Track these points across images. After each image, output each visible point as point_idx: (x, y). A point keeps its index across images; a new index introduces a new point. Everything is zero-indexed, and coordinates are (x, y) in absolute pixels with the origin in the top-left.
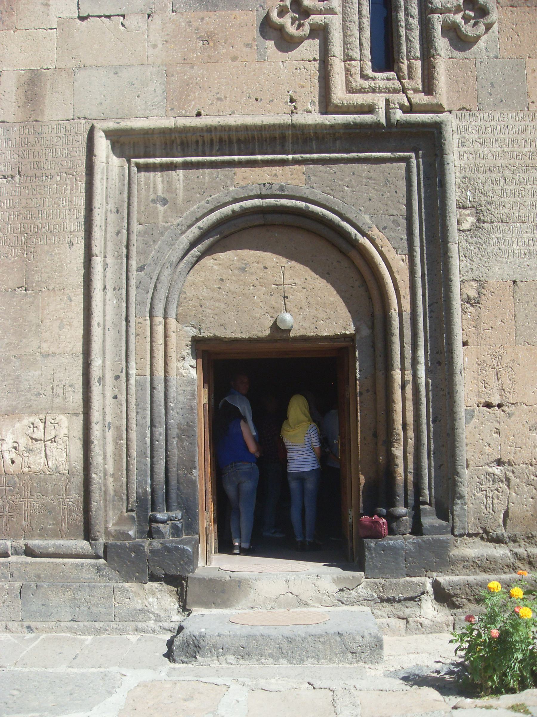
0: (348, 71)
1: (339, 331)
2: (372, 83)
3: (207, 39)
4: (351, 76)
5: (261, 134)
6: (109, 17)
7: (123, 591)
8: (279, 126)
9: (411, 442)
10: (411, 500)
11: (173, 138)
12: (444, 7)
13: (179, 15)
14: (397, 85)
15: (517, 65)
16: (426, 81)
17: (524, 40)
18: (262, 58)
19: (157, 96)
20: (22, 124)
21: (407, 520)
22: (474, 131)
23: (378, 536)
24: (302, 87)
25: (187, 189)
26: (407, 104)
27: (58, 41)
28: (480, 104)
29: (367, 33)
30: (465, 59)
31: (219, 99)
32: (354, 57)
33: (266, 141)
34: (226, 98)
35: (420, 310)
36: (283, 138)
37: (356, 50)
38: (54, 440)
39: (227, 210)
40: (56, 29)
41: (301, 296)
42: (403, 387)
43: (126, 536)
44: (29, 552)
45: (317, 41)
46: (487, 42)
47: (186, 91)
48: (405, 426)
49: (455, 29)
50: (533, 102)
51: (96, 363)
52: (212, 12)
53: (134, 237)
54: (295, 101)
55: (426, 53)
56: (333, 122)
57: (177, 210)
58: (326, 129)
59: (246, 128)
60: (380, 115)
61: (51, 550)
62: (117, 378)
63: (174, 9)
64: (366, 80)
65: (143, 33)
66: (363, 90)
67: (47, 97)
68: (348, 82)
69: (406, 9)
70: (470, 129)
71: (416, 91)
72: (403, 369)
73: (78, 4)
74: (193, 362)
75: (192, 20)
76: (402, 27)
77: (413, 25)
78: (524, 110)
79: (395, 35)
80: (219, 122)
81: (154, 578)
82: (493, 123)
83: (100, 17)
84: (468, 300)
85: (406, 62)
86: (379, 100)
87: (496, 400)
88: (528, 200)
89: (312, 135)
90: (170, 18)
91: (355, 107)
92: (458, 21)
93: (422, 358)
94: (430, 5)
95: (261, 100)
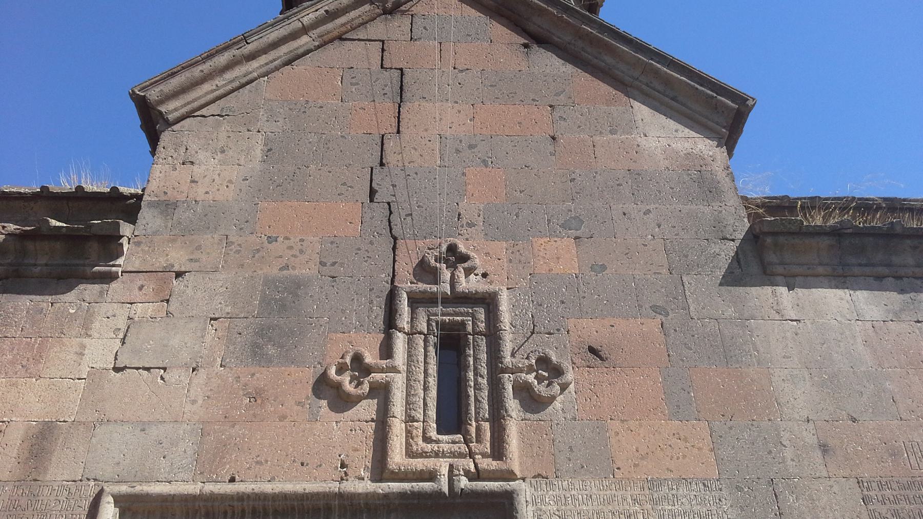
0: (409, 434)
3: (255, 396)
4: (413, 439)
5: (302, 504)
6: (148, 369)
8: (324, 495)
11: (197, 507)
12: (515, 367)
13: (228, 369)
14: (464, 448)
15: (598, 427)
16: (496, 444)
17: (604, 400)
18: (314, 418)
19: (187, 458)
20: (17, 484)
22: (551, 503)
24: (356, 450)
26: (472, 468)
27: (83, 392)
28: (558, 470)
29: (433, 393)
30: (540, 421)
31: (257, 463)
32: (416, 418)
33: (308, 511)
34: (267, 461)
37: (419, 410)
40: (85, 379)
45: (376, 401)
46: (563, 402)
47: (222, 452)
49: (528, 389)
50: (618, 468)
52: (265, 368)
54: (346, 466)
55: (496, 414)
56: (387, 490)
58: (379, 499)
59: (285, 496)
60: (443, 483)
63: (223, 363)
64: (428, 444)
65: (183, 388)
66: (424, 455)
67: (56, 453)
68: (408, 445)
69: (475, 369)
70: (547, 500)
71: (484, 455)
73: (116, 355)
75: (241, 376)
76: (471, 387)
77: (482, 385)
78: (610, 478)
79: (463, 395)
80: (253, 489)
82: (573, 492)
83: (137, 369)
85: (474, 424)
86: (441, 466)
89: (363, 506)
90: (218, 373)
91: (414, 473)
92: (530, 381)
94: (500, 365)
95: (307, 465)
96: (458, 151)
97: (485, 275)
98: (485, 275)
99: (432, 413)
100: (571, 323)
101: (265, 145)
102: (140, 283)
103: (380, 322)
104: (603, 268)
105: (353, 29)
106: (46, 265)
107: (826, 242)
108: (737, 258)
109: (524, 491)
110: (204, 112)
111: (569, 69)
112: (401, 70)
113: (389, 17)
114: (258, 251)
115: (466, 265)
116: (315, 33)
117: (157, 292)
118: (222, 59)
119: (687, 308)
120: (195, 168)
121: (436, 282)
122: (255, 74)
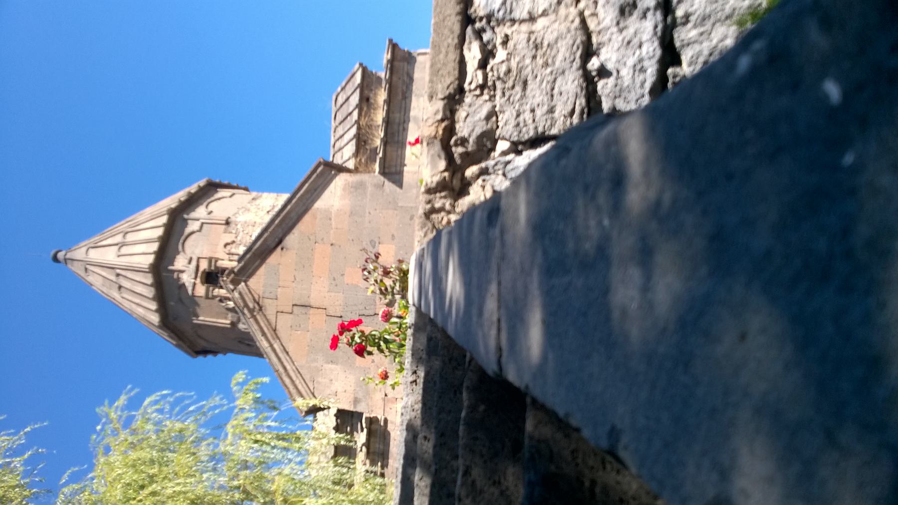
96: (336, 285)
101: (329, 363)
102: (389, 409)
104: (393, 236)
105: (270, 324)
106: (379, 444)
107: (389, 148)
108: (394, 182)
110: (312, 388)
112: (293, 305)
113: (263, 308)
114: (378, 366)
116: (272, 341)
117: (393, 402)
118: (287, 381)
119: (412, 207)
120: (339, 391)
122: (294, 367)
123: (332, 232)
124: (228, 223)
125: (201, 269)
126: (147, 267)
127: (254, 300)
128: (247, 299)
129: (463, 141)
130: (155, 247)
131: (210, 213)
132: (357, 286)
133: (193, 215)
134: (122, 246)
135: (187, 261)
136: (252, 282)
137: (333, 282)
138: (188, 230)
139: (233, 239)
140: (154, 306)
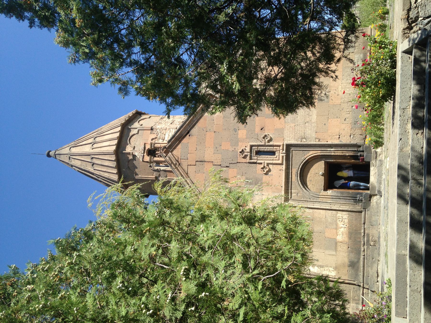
0: (275, 160)
1: (324, 164)
2: (278, 156)
7: (372, 206)
9: (346, 152)
10: (357, 152)
14: (278, 151)
18: (272, 175)
21: (361, 153)
23: (364, 159)
25: (295, 190)
29: (268, 156)
35: (320, 149)
36: (287, 172)
38: (342, 217)
39: (300, 183)
41: (316, 170)
42: (335, 153)
43: (361, 205)
44: (364, 224)
48: (342, 153)
51: (327, 208)
53: (304, 200)
57: (300, 192)
59: (285, 178)
61: (364, 219)
62: (331, 205)
68: (277, 160)
72: (331, 153)
74: (328, 191)
81: (370, 200)
84: (319, 141)
87: (338, 136)
88: (301, 129)
93: (330, 149)
96: (218, 151)
97: (246, 147)
98: (246, 147)
99: (272, 156)
100: (256, 133)
103: (256, 164)
109: (286, 142)
111: (196, 127)
115: (244, 150)
121: (247, 155)
123: (214, 126)
124: (152, 129)
125: (147, 148)
126: (113, 151)
127: (176, 159)
128: (173, 160)
129: (412, 18)
130: (116, 142)
131: (142, 125)
132: (228, 150)
133: (132, 126)
134: (94, 144)
135: (133, 148)
136: (175, 152)
137: (216, 149)
138: (131, 134)
139: (156, 136)
140: (115, 171)
